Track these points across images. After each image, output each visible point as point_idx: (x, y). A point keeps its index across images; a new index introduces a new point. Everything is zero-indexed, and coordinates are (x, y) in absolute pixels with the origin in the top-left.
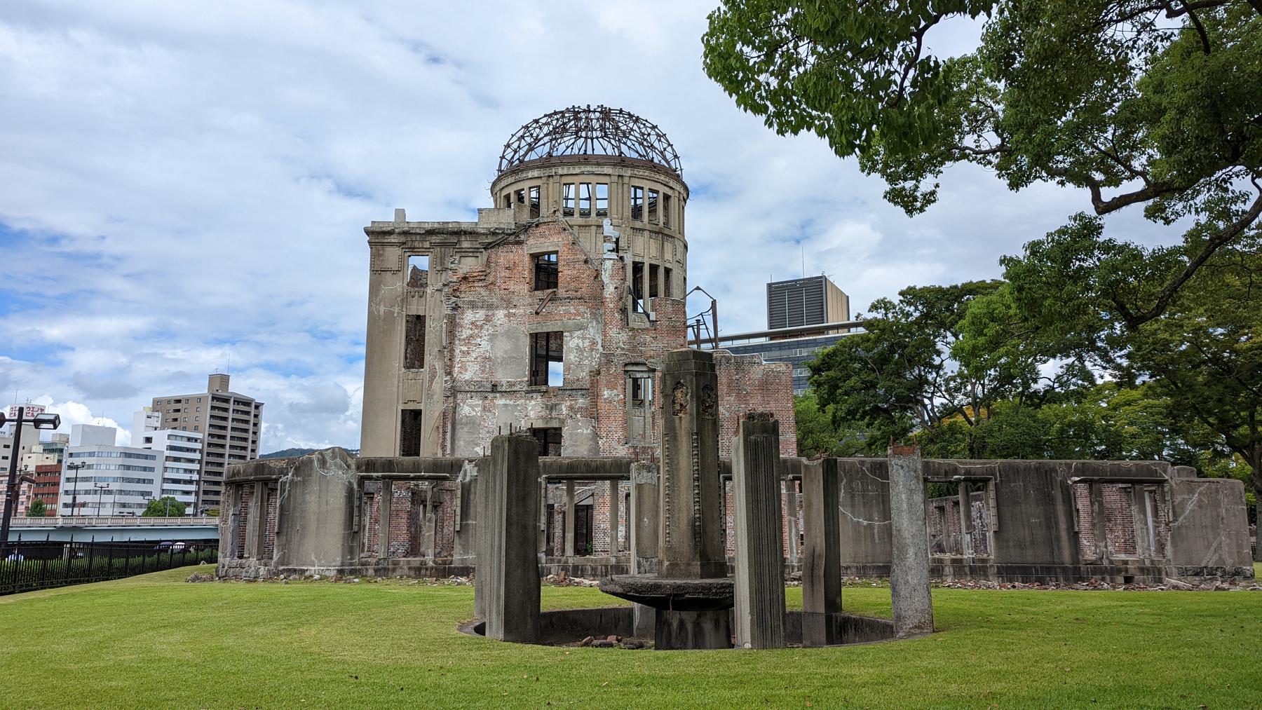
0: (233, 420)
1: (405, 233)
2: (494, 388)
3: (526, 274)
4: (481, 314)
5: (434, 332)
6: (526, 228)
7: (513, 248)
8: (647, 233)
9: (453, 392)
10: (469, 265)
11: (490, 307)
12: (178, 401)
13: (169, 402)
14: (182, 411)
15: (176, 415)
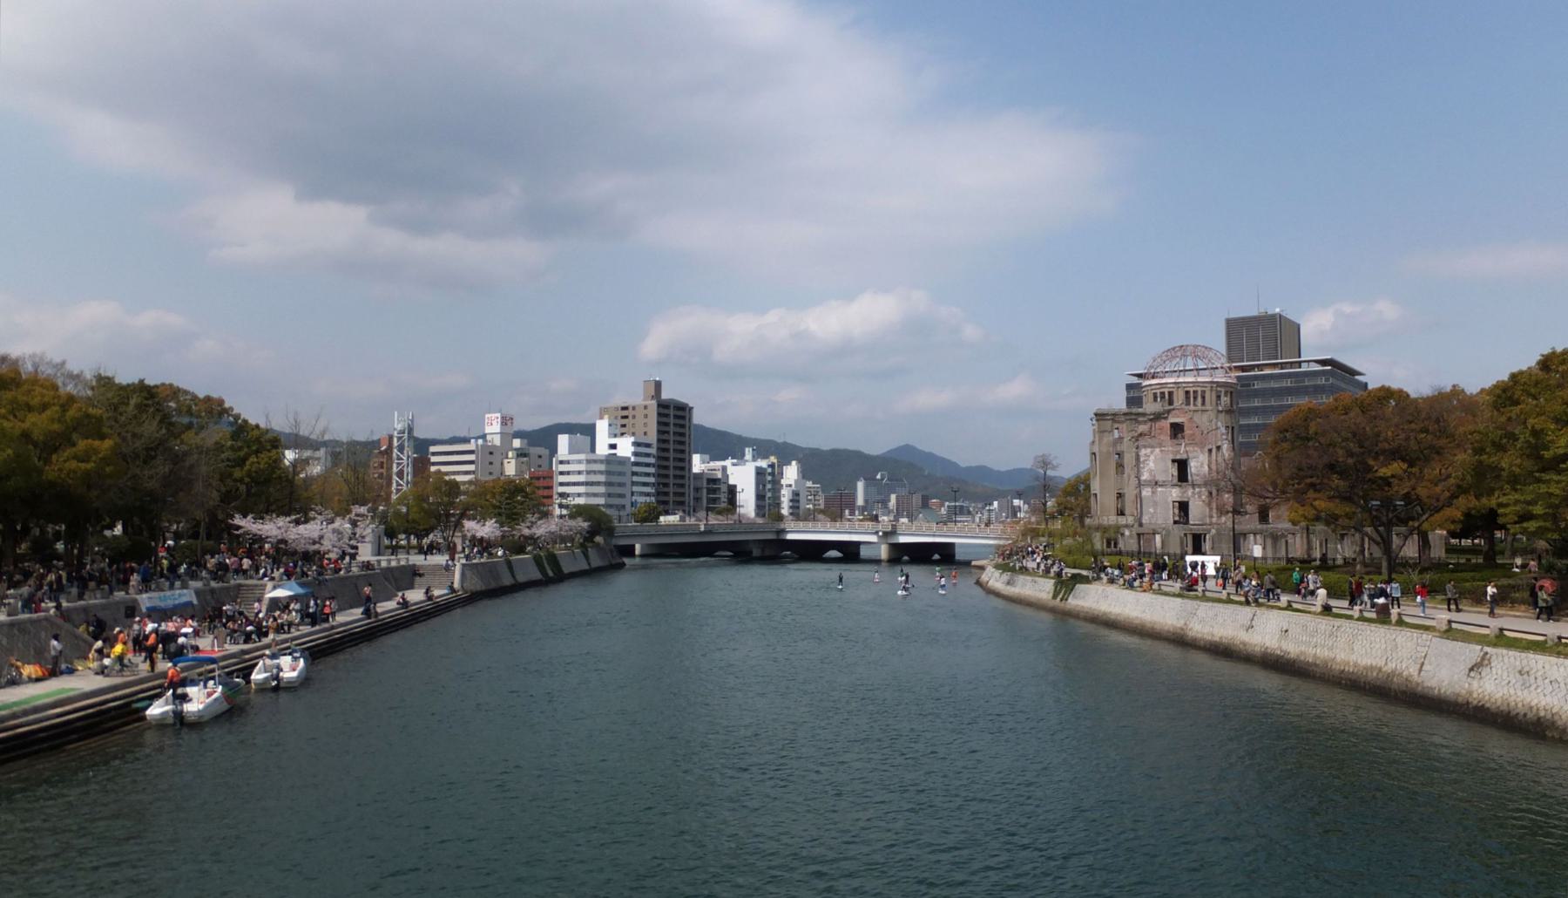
0: (675, 425)
1: (1113, 415)
2: (1156, 483)
3: (1169, 432)
4: (1149, 450)
5: (1128, 459)
6: (1169, 412)
7: (1163, 420)
8: (1223, 414)
9: (1140, 485)
10: (1142, 428)
11: (1152, 447)
12: (625, 408)
13: (616, 409)
14: (630, 417)
15: (624, 421)
